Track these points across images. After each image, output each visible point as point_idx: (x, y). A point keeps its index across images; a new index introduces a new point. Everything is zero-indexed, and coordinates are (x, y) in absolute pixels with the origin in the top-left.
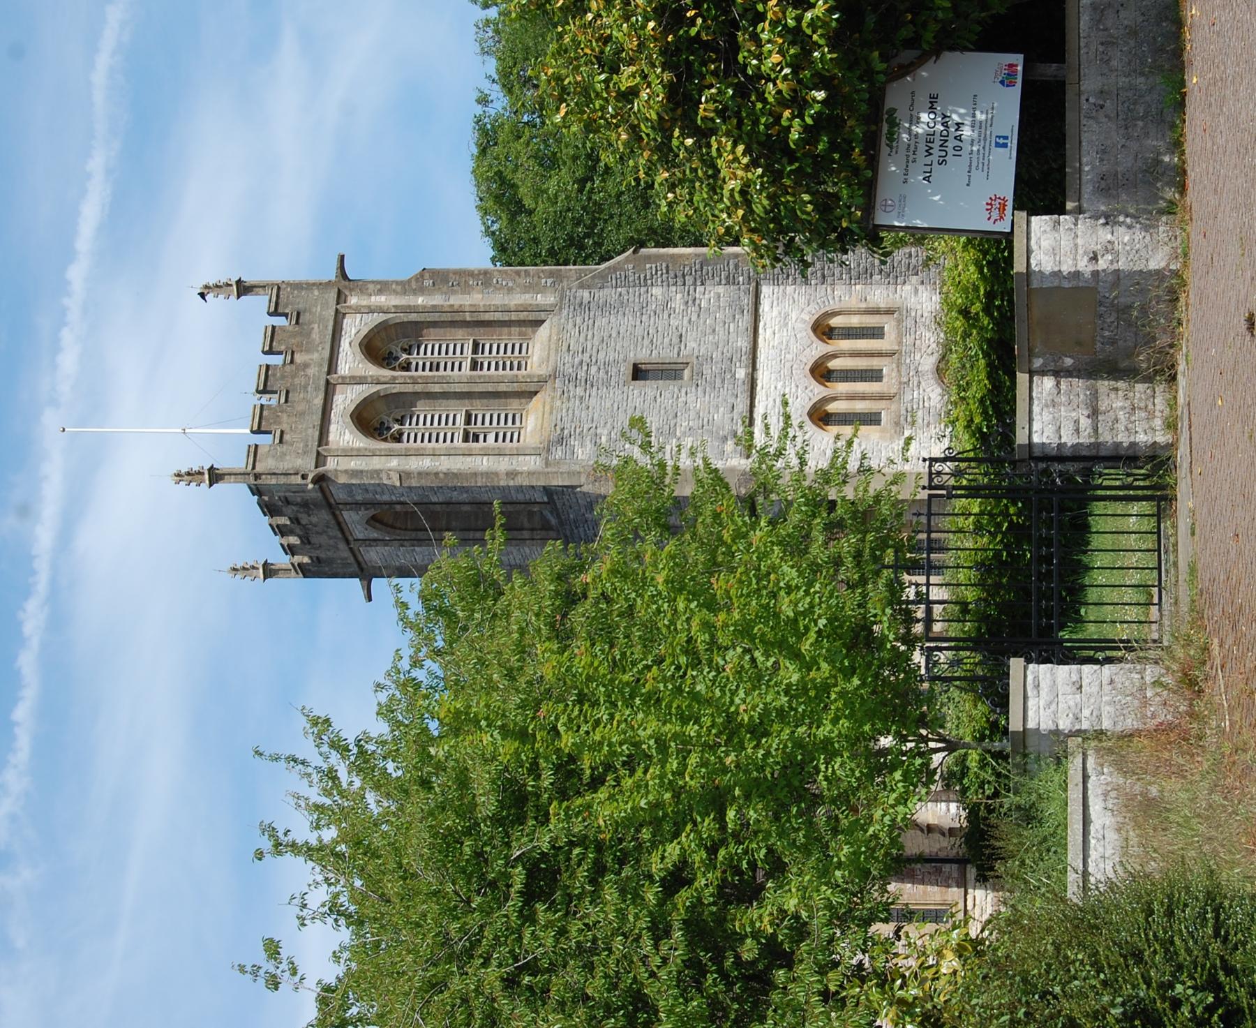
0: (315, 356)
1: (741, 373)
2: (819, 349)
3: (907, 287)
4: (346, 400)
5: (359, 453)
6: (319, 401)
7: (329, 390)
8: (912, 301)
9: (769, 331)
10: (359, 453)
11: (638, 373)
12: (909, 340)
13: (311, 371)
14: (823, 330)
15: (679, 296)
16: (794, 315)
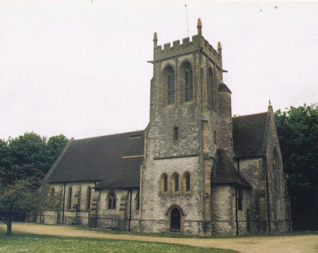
0: (181, 51)
1: (175, 155)
2: (181, 173)
3: (198, 197)
4: (172, 62)
5: (160, 69)
6: (170, 56)
7: (173, 57)
8: (194, 198)
9: (185, 160)
10: (160, 69)
11: (176, 129)
12: (184, 198)
13: (178, 52)
14: (187, 175)
15: (196, 135)
16: (190, 166)
